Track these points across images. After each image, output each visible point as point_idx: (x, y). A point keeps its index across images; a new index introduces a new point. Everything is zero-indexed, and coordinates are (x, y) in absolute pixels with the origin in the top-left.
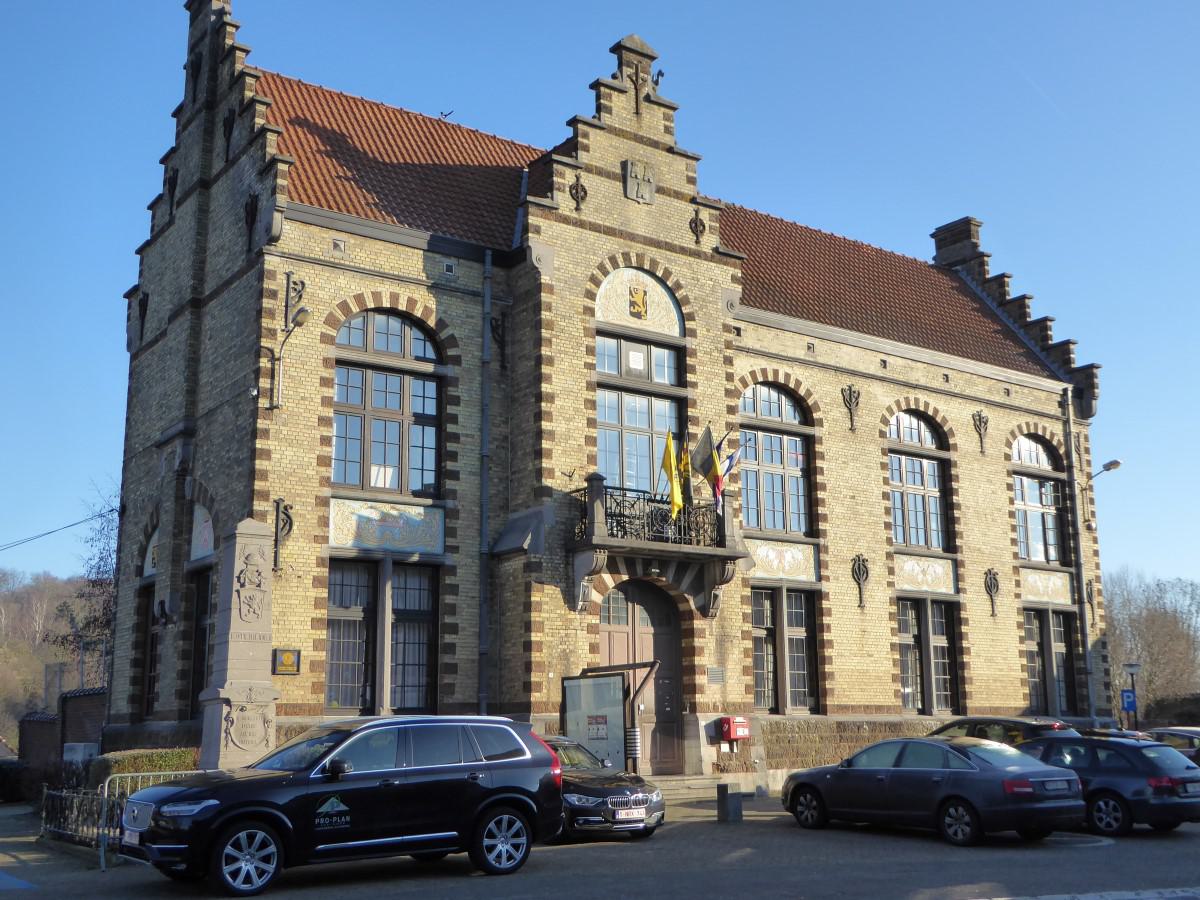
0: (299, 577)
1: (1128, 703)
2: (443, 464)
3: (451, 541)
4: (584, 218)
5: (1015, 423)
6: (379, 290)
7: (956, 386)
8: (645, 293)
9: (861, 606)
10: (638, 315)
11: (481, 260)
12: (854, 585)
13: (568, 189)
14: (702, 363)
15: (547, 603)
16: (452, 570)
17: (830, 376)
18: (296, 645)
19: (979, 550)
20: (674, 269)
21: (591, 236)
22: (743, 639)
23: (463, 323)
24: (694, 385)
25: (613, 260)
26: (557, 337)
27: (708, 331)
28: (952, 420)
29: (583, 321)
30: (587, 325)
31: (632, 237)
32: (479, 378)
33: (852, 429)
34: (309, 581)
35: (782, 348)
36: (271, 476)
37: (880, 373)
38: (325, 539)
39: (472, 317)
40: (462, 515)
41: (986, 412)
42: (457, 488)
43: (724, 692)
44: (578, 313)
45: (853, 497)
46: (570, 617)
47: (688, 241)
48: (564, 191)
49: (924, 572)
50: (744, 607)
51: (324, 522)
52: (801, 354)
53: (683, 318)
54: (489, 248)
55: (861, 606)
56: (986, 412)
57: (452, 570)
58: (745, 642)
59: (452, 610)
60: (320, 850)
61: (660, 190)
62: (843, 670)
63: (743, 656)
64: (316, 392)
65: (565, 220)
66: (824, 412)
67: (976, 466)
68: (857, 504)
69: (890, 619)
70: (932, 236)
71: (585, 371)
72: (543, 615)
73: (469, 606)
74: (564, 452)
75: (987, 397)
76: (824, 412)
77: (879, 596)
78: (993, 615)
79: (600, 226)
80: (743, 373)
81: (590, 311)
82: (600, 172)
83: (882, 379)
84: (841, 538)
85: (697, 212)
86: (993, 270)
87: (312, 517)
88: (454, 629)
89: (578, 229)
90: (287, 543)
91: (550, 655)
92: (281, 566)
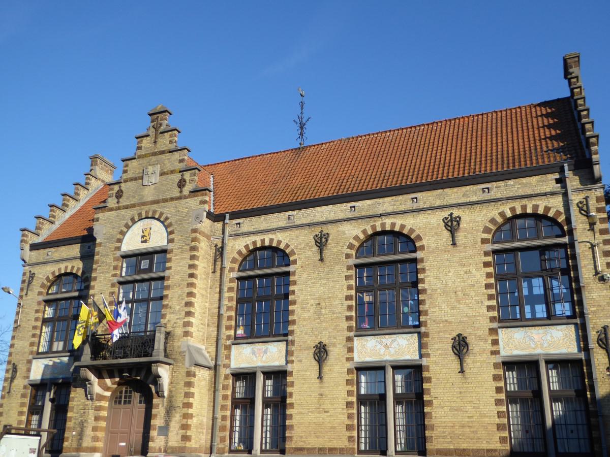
4: (121, 205)
8: (151, 229)
9: (320, 377)
10: (145, 242)
12: (315, 363)
14: (176, 255)
19: (446, 321)
20: (165, 211)
21: (123, 212)
22: (183, 408)
26: (100, 266)
27: (182, 236)
28: (420, 228)
29: (113, 254)
30: (115, 256)
31: (144, 204)
33: (322, 260)
38: (28, 377)
41: (456, 212)
43: (167, 442)
44: (112, 251)
45: (319, 304)
46: (87, 403)
49: (387, 346)
51: (29, 370)
52: (282, 224)
53: (170, 233)
54: (227, 213)
55: (320, 377)
56: (456, 212)
58: (184, 409)
62: (301, 424)
65: (111, 210)
66: (298, 254)
77: (337, 366)
78: (462, 371)
79: (128, 205)
80: (240, 248)
82: (131, 179)
84: (306, 334)
89: (117, 211)
92: (12, 391)
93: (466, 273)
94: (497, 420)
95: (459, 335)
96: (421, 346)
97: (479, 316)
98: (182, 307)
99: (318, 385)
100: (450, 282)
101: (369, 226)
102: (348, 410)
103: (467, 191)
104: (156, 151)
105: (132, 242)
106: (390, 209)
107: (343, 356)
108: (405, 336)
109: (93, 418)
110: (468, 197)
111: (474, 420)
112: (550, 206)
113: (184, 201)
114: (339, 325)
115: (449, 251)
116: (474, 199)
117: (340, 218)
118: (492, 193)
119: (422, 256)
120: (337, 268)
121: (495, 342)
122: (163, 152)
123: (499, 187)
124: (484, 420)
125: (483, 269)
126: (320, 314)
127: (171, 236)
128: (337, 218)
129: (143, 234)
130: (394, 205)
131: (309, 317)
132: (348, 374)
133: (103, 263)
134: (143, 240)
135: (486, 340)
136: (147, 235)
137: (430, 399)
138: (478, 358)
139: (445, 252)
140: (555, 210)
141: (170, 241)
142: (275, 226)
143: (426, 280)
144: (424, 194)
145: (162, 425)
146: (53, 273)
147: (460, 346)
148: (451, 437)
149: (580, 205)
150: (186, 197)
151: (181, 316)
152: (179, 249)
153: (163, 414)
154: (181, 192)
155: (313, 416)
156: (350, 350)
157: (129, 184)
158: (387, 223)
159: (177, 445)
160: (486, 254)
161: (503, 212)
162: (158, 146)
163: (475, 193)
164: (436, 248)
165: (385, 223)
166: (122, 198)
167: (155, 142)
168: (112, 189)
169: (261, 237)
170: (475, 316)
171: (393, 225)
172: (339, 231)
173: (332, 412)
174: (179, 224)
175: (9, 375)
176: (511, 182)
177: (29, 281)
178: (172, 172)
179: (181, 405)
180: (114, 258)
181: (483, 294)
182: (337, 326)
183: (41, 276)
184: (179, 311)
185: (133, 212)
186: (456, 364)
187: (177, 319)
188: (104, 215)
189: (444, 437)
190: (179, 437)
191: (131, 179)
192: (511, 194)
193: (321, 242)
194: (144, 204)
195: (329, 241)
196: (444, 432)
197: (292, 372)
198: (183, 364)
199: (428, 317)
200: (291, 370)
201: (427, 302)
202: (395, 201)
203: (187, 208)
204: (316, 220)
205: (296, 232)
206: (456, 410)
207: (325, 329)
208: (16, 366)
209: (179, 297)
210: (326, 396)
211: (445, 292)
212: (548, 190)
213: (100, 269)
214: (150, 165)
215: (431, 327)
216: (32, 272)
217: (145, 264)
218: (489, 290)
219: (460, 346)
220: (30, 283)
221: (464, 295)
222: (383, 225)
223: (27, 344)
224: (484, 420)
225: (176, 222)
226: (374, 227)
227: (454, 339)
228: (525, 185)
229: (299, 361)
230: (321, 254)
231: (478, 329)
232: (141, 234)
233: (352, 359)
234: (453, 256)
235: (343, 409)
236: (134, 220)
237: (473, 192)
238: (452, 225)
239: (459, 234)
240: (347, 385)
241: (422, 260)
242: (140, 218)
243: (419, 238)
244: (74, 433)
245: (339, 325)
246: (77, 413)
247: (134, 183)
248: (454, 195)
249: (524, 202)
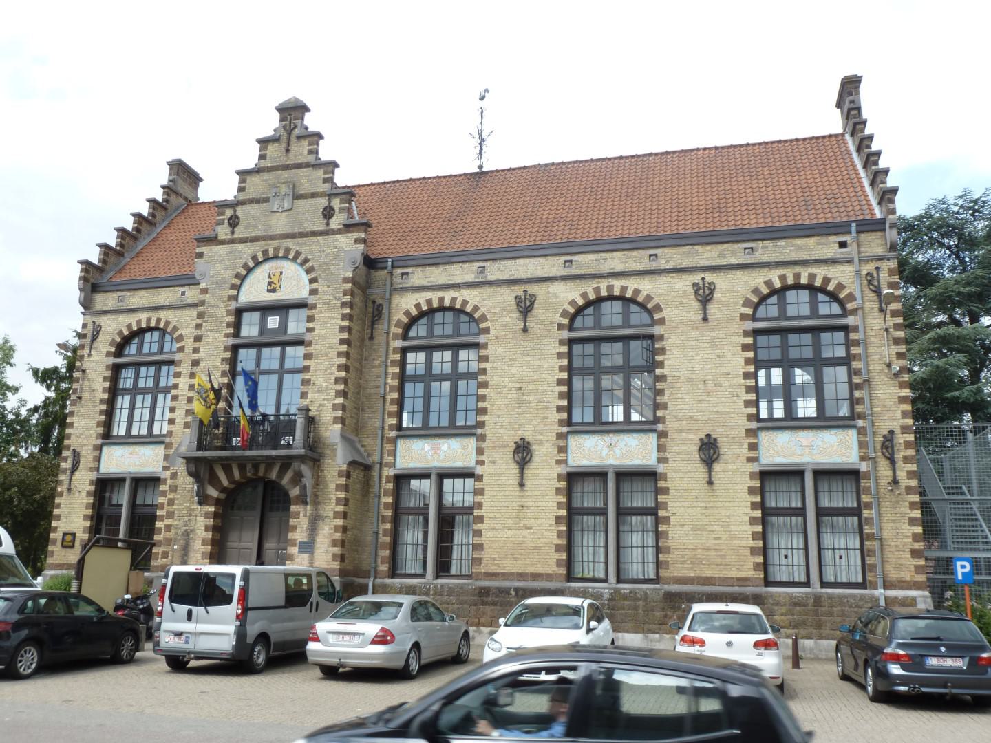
1: (963, 574)
4: (236, 236)
7: (667, 262)
8: (281, 273)
9: (522, 485)
10: (273, 291)
13: (226, 221)
14: (321, 313)
15: (178, 499)
17: (504, 290)
18: (74, 531)
21: (239, 247)
22: (334, 518)
26: (206, 321)
27: (329, 286)
28: (660, 296)
29: (226, 306)
31: (272, 238)
33: (525, 330)
34: (84, 494)
35: (449, 278)
37: (564, 273)
38: (98, 469)
41: (710, 277)
44: (225, 301)
45: (520, 389)
47: (319, 225)
48: (223, 224)
50: (338, 493)
51: (98, 459)
52: (470, 278)
53: (312, 281)
55: (522, 485)
58: (336, 520)
61: (297, 197)
62: (493, 542)
63: (332, 531)
65: (222, 242)
66: (492, 321)
67: (694, 334)
69: (557, 495)
72: (175, 507)
76: (492, 321)
78: (710, 483)
79: (247, 238)
82: (251, 201)
83: (563, 278)
84: (501, 426)
85: (329, 202)
91: (176, 533)
93: (719, 357)
94: (752, 542)
95: (708, 436)
96: (661, 448)
97: (734, 413)
98: (331, 384)
100: (697, 368)
101: (591, 288)
102: (558, 526)
103: (724, 250)
104: (288, 163)
105: (255, 291)
106: (619, 267)
107: (551, 458)
108: (635, 435)
109: (203, 528)
110: (725, 257)
111: (722, 542)
112: (829, 276)
113: (331, 238)
114: (547, 418)
115: (697, 328)
116: (733, 261)
117: (551, 275)
118: (757, 254)
119: (662, 333)
120: (546, 341)
121: (753, 447)
122: (298, 166)
123: (767, 247)
124: (734, 542)
125: (741, 353)
126: (521, 402)
127: (315, 286)
128: (546, 275)
129: (270, 280)
130: (626, 262)
131: (507, 407)
132: (559, 481)
133: (211, 316)
134: (269, 288)
135: (741, 444)
136: (276, 282)
137: (666, 515)
138: (731, 466)
139: (693, 328)
140: (836, 282)
141: (313, 292)
142: (458, 280)
143: (667, 364)
144: (666, 250)
145: (305, 540)
146: (129, 326)
147: (709, 450)
148: (692, 563)
149: (869, 278)
150: (334, 232)
151: (329, 397)
152: (325, 303)
153: (305, 526)
154: (328, 224)
155: (510, 532)
156: (563, 450)
157: (248, 207)
158: (615, 286)
159: (326, 566)
160: (746, 334)
161: (770, 280)
162: (291, 155)
163: (734, 253)
164: (681, 323)
165: (613, 286)
166: (238, 227)
167: (288, 151)
168: (223, 214)
169: (440, 294)
170: (729, 413)
171: (624, 289)
172: (548, 293)
173: (535, 528)
174: (325, 270)
176: (782, 243)
177: (93, 336)
178: (314, 195)
179: (331, 514)
180: (228, 311)
181: (740, 385)
182: (544, 418)
183: (110, 330)
184: (327, 388)
185: (256, 248)
186: (701, 473)
187: (324, 400)
188: (211, 250)
189: (683, 562)
190: (330, 556)
191: (251, 201)
192: (781, 258)
193: (525, 307)
194: (272, 238)
195: (536, 306)
196: (683, 556)
197: (482, 475)
198: (334, 461)
199: (668, 412)
200: (481, 473)
201: (667, 392)
202: (627, 257)
203: (336, 248)
204: (517, 276)
205: (488, 291)
206: (699, 529)
207: (529, 421)
209: (326, 371)
210: (528, 508)
211: (690, 381)
212: (829, 256)
213: (206, 326)
214: (280, 183)
215: (670, 425)
216: (97, 323)
217: (273, 322)
218: (748, 381)
219: (709, 450)
220: (94, 338)
221: (715, 385)
222: (610, 288)
224: (734, 542)
225: (320, 266)
226: (597, 290)
227: (701, 440)
228: (800, 247)
229: (490, 462)
230: (525, 322)
231: (732, 429)
232: (267, 280)
233: (565, 462)
234: (703, 335)
235: (551, 525)
236: (257, 259)
237: (733, 253)
238: (705, 296)
239: (712, 306)
240: (557, 495)
241: (661, 338)
242: (266, 257)
243: (658, 308)
244: (176, 547)
245: (547, 418)
247: (255, 207)
248: (707, 255)
249: (797, 269)
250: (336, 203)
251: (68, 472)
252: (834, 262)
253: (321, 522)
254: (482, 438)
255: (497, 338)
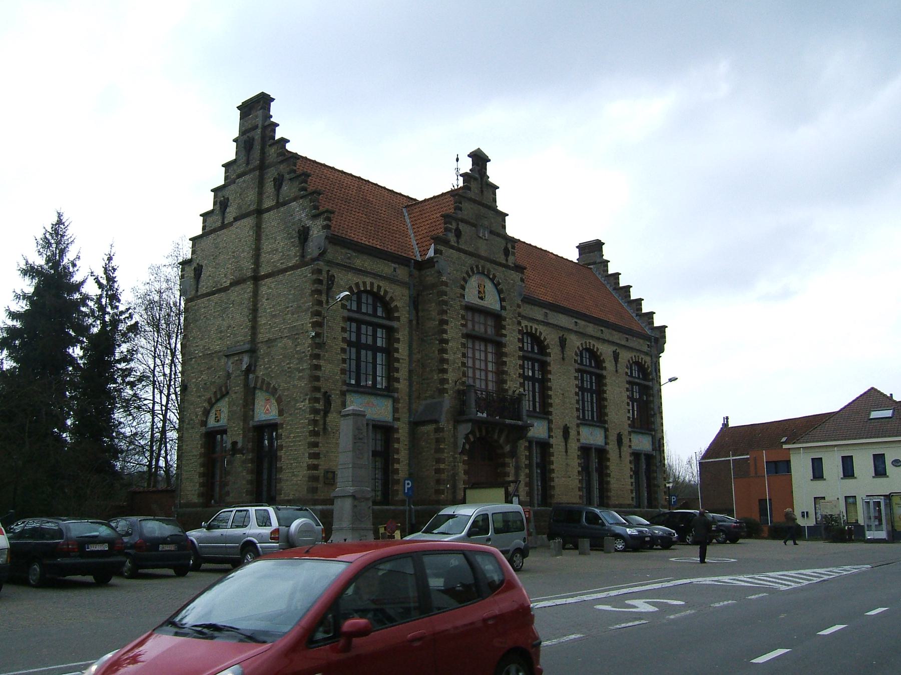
0: (334, 433)
2: (392, 374)
3: (396, 415)
5: (630, 356)
6: (365, 280)
8: (484, 287)
9: (566, 452)
10: (481, 298)
11: (408, 266)
13: (453, 231)
15: (445, 449)
16: (397, 430)
20: (497, 274)
21: (463, 256)
23: (401, 299)
24: (505, 336)
25: (472, 269)
27: (511, 307)
29: (459, 301)
30: (462, 303)
31: (479, 257)
32: (407, 329)
33: (563, 359)
36: (322, 379)
39: (405, 296)
40: (401, 401)
42: (399, 387)
44: (458, 297)
45: (563, 394)
48: (452, 232)
52: (540, 317)
53: (502, 300)
55: (566, 452)
57: (397, 430)
59: (397, 451)
60: (674, 530)
64: (340, 335)
65: (452, 247)
68: (565, 398)
70: (577, 247)
71: (461, 328)
73: (405, 450)
74: (453, 370)
75: (618, 342)
77: (574, 446)
78: (620, 457)
81: (463, 296)
83: (576, 332)
86: (611, 271)
87: (339, 401)
88: (398, 461)
90: (329, 415)
96: (606, 437)
99: (564, 457)
106: (592, 333)
109: (463, 472)
121: (630, 440)
127: (504, 304)
133: (451, 306)
141: (503, 308)
175: (319, 406)
177: (328, 284)
200: (552, 443)
208: (330, 396)
210: (569, 465)
223: (337, 370)
229: (556, 437)
230: (563, 354)
238: (616, 356)
246: (449, 466)
248: (616, 337)
250: (509, 246)
251: (322, 413)
252: (646, 354)
253: (520, 471)
254: (550, 422)
255: (554, 361)
